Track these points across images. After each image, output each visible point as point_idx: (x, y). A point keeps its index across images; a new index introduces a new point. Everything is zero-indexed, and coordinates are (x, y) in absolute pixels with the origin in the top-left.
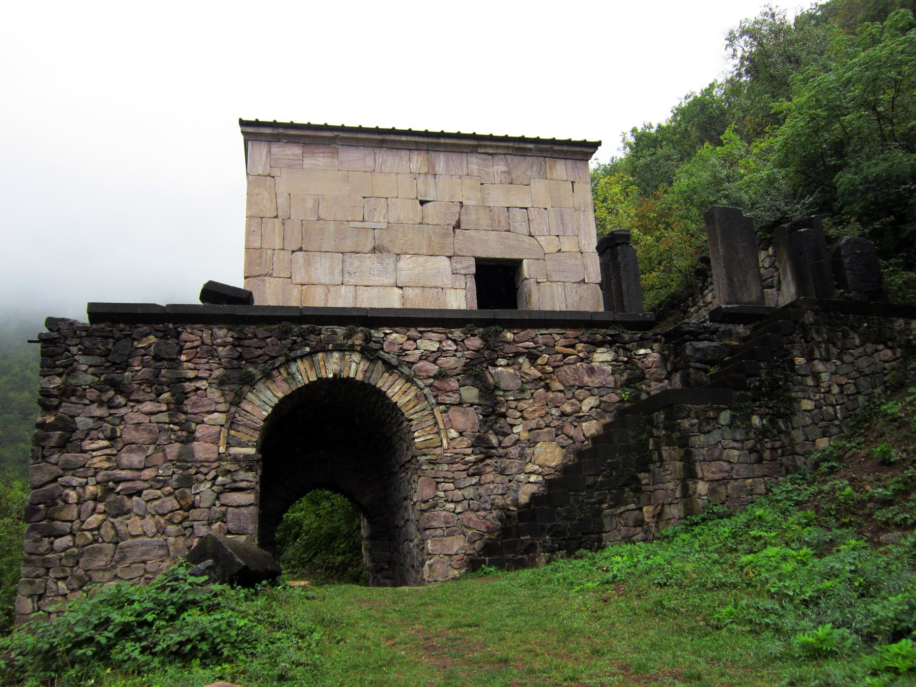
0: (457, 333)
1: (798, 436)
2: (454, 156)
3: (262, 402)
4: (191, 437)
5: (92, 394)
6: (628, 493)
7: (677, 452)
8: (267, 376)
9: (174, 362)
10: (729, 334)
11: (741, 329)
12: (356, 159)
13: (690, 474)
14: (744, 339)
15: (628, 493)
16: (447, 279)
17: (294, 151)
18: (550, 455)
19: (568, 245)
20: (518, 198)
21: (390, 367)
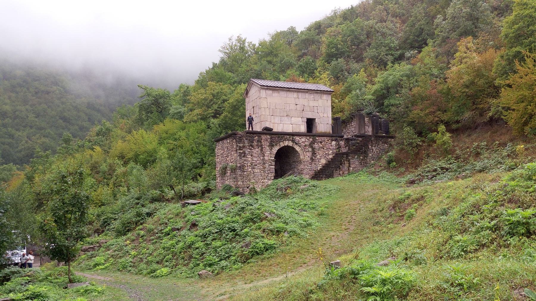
0: (308, 138)
1: (368, 160)
2: (303, 94)
3: (275, 149)
4: (264, 156)
5: (248, 147)
6: (338, 169)
7: (348, 162)
8: (276, 145)
9: (261, 142)
10: (358, 140)
11: (360, 139)
12: (283, 94)
13: (350, 166)
14: (361, 141)
15: (338, 169)
16: (301, 123)
17: (271, 92)
18: (323, 161)
19: (325, 115)
20: (315, 104)
21: (296, 144)
